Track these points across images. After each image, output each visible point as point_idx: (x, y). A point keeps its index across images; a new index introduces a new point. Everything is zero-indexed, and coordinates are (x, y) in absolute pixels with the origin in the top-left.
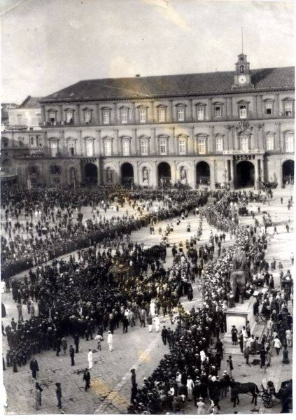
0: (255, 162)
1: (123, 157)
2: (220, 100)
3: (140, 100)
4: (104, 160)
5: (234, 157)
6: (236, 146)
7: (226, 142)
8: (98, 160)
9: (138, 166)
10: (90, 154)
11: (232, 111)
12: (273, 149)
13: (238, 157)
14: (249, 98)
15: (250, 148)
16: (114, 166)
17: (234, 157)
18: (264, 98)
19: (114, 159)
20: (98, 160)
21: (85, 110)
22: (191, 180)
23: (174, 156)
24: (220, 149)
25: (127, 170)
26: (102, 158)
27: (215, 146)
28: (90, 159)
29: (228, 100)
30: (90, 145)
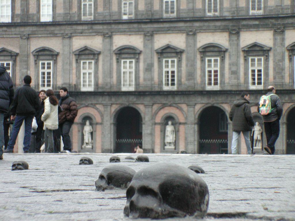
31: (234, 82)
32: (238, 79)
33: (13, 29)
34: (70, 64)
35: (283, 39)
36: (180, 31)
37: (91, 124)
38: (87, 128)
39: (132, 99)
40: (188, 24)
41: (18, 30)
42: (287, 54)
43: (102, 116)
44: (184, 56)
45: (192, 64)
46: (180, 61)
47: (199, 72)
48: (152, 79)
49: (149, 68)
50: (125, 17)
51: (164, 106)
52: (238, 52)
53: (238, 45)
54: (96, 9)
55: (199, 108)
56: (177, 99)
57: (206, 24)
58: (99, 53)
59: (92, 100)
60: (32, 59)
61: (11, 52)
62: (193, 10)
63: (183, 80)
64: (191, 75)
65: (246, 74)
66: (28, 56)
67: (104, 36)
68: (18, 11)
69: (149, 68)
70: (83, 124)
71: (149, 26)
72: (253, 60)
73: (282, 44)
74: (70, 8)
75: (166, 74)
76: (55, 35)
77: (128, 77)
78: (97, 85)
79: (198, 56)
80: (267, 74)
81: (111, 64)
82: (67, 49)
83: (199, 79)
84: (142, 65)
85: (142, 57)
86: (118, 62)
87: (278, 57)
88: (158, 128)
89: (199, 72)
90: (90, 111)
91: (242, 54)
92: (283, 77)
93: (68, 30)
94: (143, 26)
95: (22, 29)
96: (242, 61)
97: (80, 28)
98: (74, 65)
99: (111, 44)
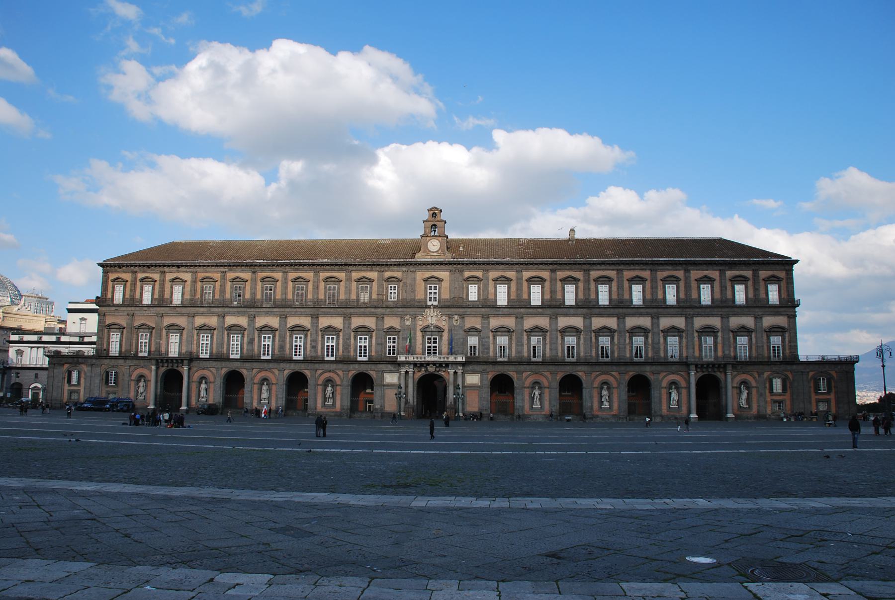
6: (419, 348)
8: (186, 362)
9: (252, 379)
10: (174, 351)
11: (413, 291)
14: (444, 274)
17: (415, 364)
18: (467, 274)
19: (214, 364)
20: (186, 362)
27: (381, 344)
28: (172, 360)
30: (174, 339)
31: (313, 354)
32: (316, 351)
33: (151, 309)
34: (193, 337)
35: (350, 324)
38: (203, 386)
39: (238, 364)
40: (282, 310)
41: (155, 309)
42: (352, 334)
43: (215, 377)
44: (277, 333)
45: (283, 339)
46: (274, 337)
47: (288, 346)
48: (253, 350)
49: (251, 341)
50: (235, 303)
51: (261, 370)
52: (317, 332)
53: (317, 326)
54: (214, 296)
55: (287, 372)
56: (271, 365)
57: (295, 310)
59: (208, 364)
60: (164, 331)
61: (148, 326)
62: (285, 300)
63: (276, 351)
64: (282, 348)
65: (323, 348)
66: (161, 330)
67: (219, 316)
68: (156, 296)
69: (251, 341)
70: (200, 383)
71: (253, 310)
72: (328, 338)
73: (349, 327)
74: (195, 295)
75: (267, 345)
76: (182, 315)
77: (235, 347)
78: (211, 353)
79: (288, 334)
80: (337, 349)
81: (223, 338)
82: (190, 325)
83: (287, 351)
84: (246, 339)
85: (246, 333)
86: (229, 336)
88: (256, 387)
89: (288, 346)
90: (206, 373)
91: (320, 333)
92: (349, 352)
93: (193, 310)
94: (248, 310)
95: (158, 309)
96: (320, 338)
97: (202, 309)
98: (195, 337)
99: (224, 323)
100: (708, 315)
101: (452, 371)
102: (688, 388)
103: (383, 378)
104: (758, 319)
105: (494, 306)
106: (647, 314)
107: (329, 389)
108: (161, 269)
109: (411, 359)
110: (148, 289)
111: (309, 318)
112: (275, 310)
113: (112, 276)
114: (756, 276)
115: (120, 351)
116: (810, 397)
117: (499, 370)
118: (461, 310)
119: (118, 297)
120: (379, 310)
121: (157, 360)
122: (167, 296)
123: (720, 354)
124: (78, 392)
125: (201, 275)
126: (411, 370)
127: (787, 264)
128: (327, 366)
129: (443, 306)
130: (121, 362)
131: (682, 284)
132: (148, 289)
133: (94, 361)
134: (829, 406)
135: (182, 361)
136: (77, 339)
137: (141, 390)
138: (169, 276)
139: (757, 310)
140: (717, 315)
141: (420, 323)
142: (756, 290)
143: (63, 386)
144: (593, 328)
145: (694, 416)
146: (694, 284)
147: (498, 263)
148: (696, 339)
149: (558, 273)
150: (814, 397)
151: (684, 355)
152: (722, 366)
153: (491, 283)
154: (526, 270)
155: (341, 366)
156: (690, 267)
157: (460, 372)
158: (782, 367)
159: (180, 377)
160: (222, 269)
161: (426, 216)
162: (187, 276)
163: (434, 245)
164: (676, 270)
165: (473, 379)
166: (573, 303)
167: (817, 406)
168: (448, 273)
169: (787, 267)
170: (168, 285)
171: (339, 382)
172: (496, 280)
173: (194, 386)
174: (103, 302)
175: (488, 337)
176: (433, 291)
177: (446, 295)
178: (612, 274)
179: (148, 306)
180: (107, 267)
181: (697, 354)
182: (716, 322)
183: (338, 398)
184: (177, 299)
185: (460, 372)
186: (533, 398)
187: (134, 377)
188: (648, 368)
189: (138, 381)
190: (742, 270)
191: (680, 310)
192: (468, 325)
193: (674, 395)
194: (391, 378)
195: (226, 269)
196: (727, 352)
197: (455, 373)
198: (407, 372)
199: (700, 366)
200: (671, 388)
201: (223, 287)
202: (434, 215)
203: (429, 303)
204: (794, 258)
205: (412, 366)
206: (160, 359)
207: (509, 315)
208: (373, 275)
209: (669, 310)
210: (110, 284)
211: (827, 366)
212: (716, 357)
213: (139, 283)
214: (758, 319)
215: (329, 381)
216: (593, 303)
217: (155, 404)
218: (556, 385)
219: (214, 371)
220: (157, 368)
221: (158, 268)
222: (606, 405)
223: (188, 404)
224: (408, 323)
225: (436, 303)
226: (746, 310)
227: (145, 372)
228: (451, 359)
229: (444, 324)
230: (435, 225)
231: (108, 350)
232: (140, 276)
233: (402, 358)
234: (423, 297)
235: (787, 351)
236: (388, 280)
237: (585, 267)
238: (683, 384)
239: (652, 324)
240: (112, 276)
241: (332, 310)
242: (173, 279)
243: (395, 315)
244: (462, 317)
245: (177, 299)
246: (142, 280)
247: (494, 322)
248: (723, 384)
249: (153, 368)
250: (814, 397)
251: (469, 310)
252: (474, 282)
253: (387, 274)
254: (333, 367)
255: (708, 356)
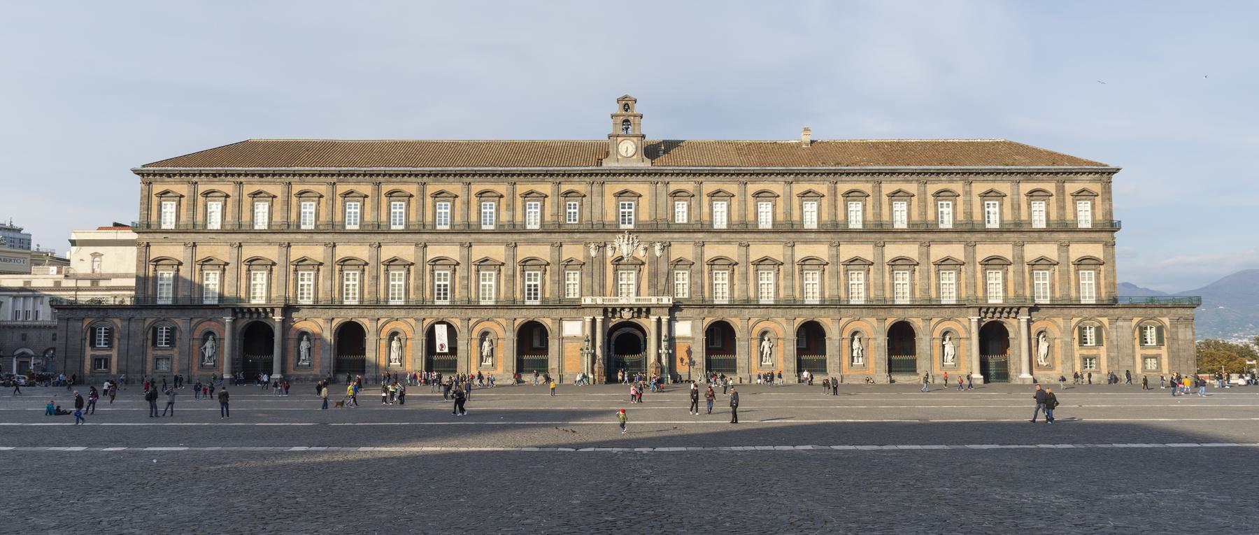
0: (649, 324)
1: (342, 306)
2: (580, 186)
3: (393, 179)
4: (294, 315)
5: (605, 310)
7: (587, 281)
9: (378, 332)
12: (686, 296)
13: (614, 310)
14: (639, 186)
15: (638, 293)
16: (322, 326)
17: (605, 310)
18: (673, 187)
21: (256, 195)
22: (502, 366)
23: (377, 305)
24: (573, 292)
25: (351, 336)
26: (289, 309)
27: (561, 283)
29: (596, 188)
30: (260, 278)
36: (408, 243)
37: (309, 340)
51: (391, 319)
58: (321, 264)
73: (514, 257)
87: (510, 272)
95: (233, 236)
96: (473, 276)
100: (994, 242)
101: (653, 319)
102: (969, 339)
103: (560, 328)
104: (1064, 247)
105: (1074, 230)
106: (914, 241)
107: (486, 344)
108: (236, 179)
109: (599, 301)
110: (215, 208)
111: (458, 248)
112: (408, 236)
113: (158, 188)
114: (1061, 191)
115: (175, 298)
116: (1134, 351)
117: (719, 315)
118: (667, 235)
119: (169, 222)
120: (553, 236)
121: (234, 309)
122: (246, 218)
123: (1011, 294)
124: (107, 360)
125: (297, 188)
126: (599, 319)
127: (1106, 173)
128: (484, 313)
129: (640, 230)
130: (175, 313)
131: (960, 200)
132: (215, 208)
133: (132, 313)
134: (1159, 365)
135: (273, 310)
136: (88, 284)
137: (209, 352)
138: (249, 189)
139: (1063, 235)
140: (1006, 242)
141: (609, 253)
142: (1062, 208)
143: (82, 351)
144: (842, 260)
145: (977, 376)
146: (977, 201)
147: (893, 173)
148: (979, 275)
149: (794, 186)
150: (1139, 352)
151: (964, 295)
152: (1013, 310)
153: (706, 200)
154: (753, 182)
155: (502, 312)
156: (972, 177)
157: (665, 319)
158: (1096, 311)
159: (271, 333)
160: (329, 179)
161: (617, 109)
162: (276, 189)
163: (628, 148)
164: (952, 181)
165: (683, 328)
166: (905, 226)
167: (1144, 363)
168: (647, 186)
169: (1105, 177)
170: (247, 200)
171: (501, 334)
172: (714, 195)
173: (292, 343)
174: (147, 227)
175: (702, 272)
176: (627, 210)
177: (644, 217)
178: (867, 187)
179: (216, 232)
180: (147, 174)
181: (980, 294)
182: (1006, 251)
183: (499, 354)
184: (261, 222)
185: (665, 319)
186: (762, 353)
187: (197, 334)
188: (913, 312)
189: (205, 340)
190: (1042, 181)
191: (956, 235)
192: (675, 256)
193: (949, 348)
194: (573, 328)
195: (335, 179)
196: (1020, 292)
197: (659, 320)
198: (594, 321)
199: (983, 309)
200: (944, 340)
201: (969, 203)
202: (626, 107)
203: (622, 227)
204: (1112, 165)
205: (601, 311)
206: (236, 308)
207: (729, 242)
208: (546, 188)
209: (942, 235)
210: (155, 200)
211: (1157, 311)
212: (1006, 298)
213: (201, 200)
214: (1064, 247)
215: (484, 335)
216: (841, 228)
217: (233, 372)
218: (792, 336)
219: (413, 322)
220: (234, 322)
221: (229, 178)
222: (859, 362)
223: (283, 371)
224: (593, 253)
225: (631, 227)
226: (1046, 235)
227: (213, 326)
228: (654, 301)
229: (641, 254)
230: (627, 121)
231: (155, 298)
232: (202, 188)
233: (588, 301)
234: (614, 219)
235: (1103, 291)
236: (567, 194)
237: (876, 178)
238: (963, 334)
239: (921, 254)
240: (158, 188)
241: (489, 236)
242: (1032, 192)
243: (575, 242)
244: (666, 246)
245: (261, 222)
246: (206, 194)
247: (711, 252)
248: (1011, 335)
249: (228, 319)
250: (1139, 352)
251: (677, 235)
252: (682, 198)
253: (565, 188)
254: (493, 312)
255: (996, 299)
